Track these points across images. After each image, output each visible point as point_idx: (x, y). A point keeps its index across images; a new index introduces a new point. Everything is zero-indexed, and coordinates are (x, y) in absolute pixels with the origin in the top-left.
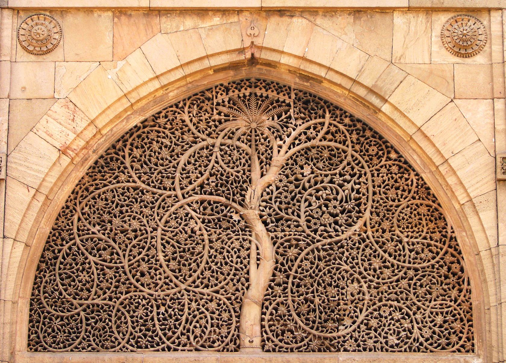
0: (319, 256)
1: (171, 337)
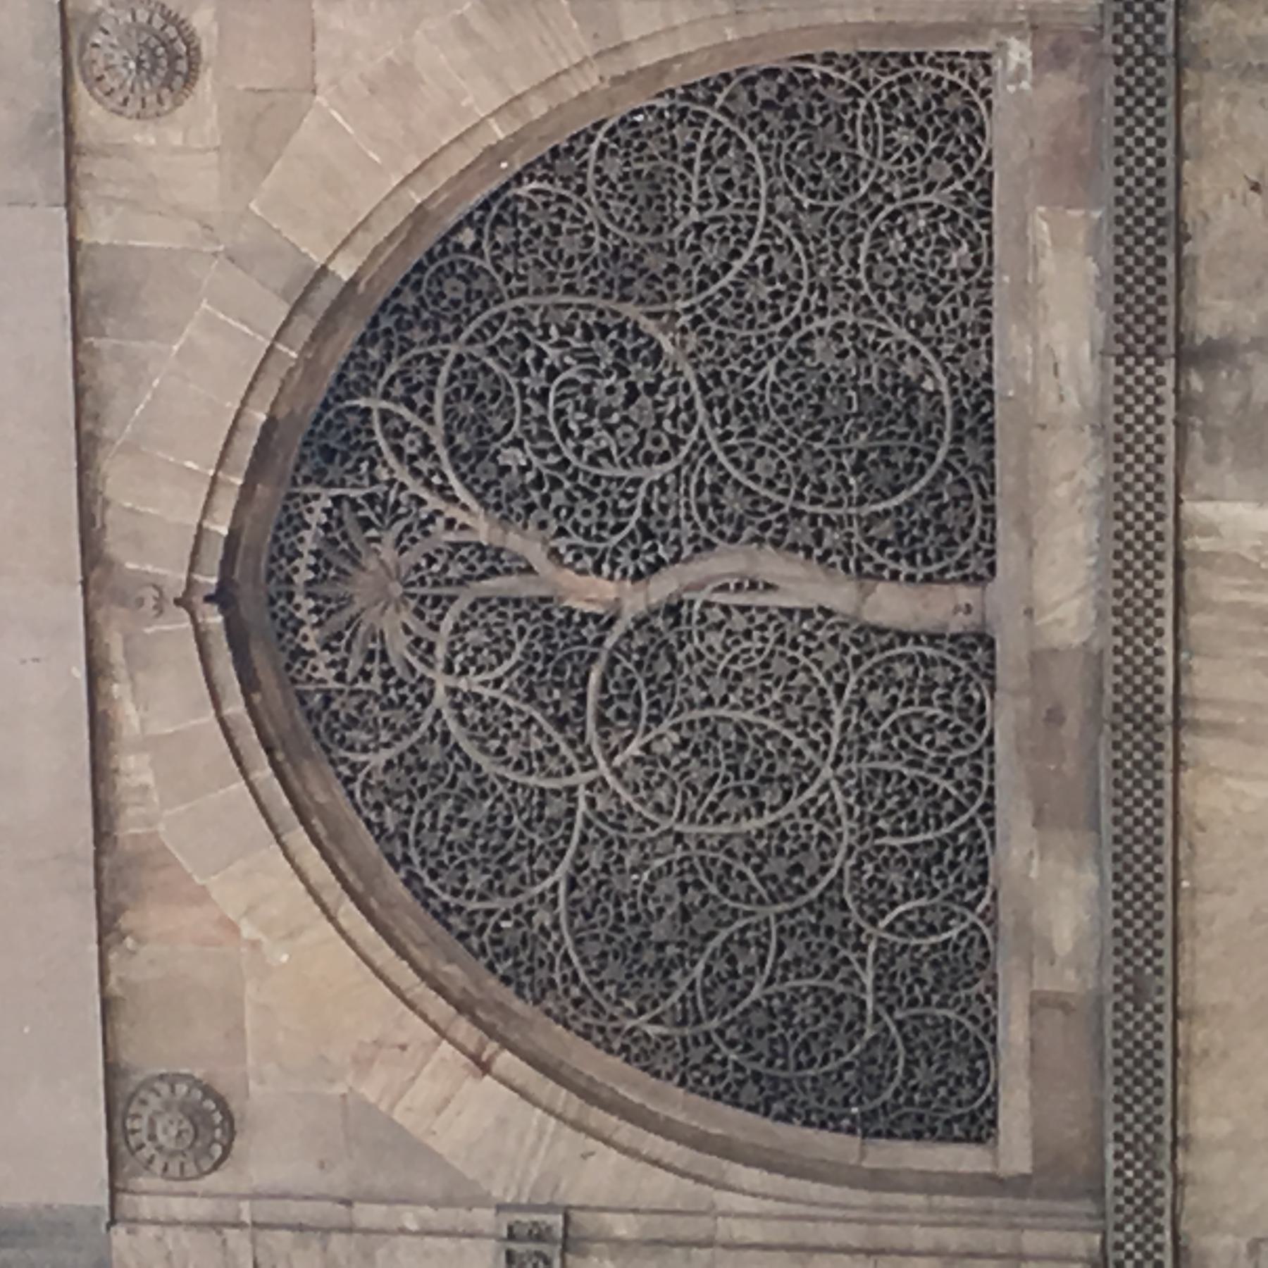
1: (958, 803)
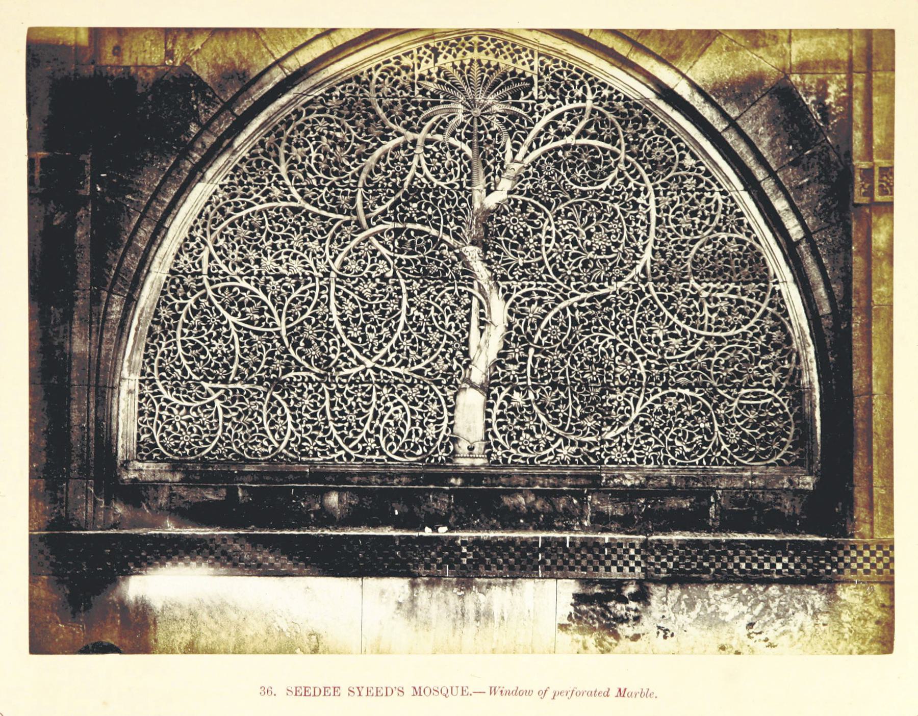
0: (573, 318)
1: (352, 440)
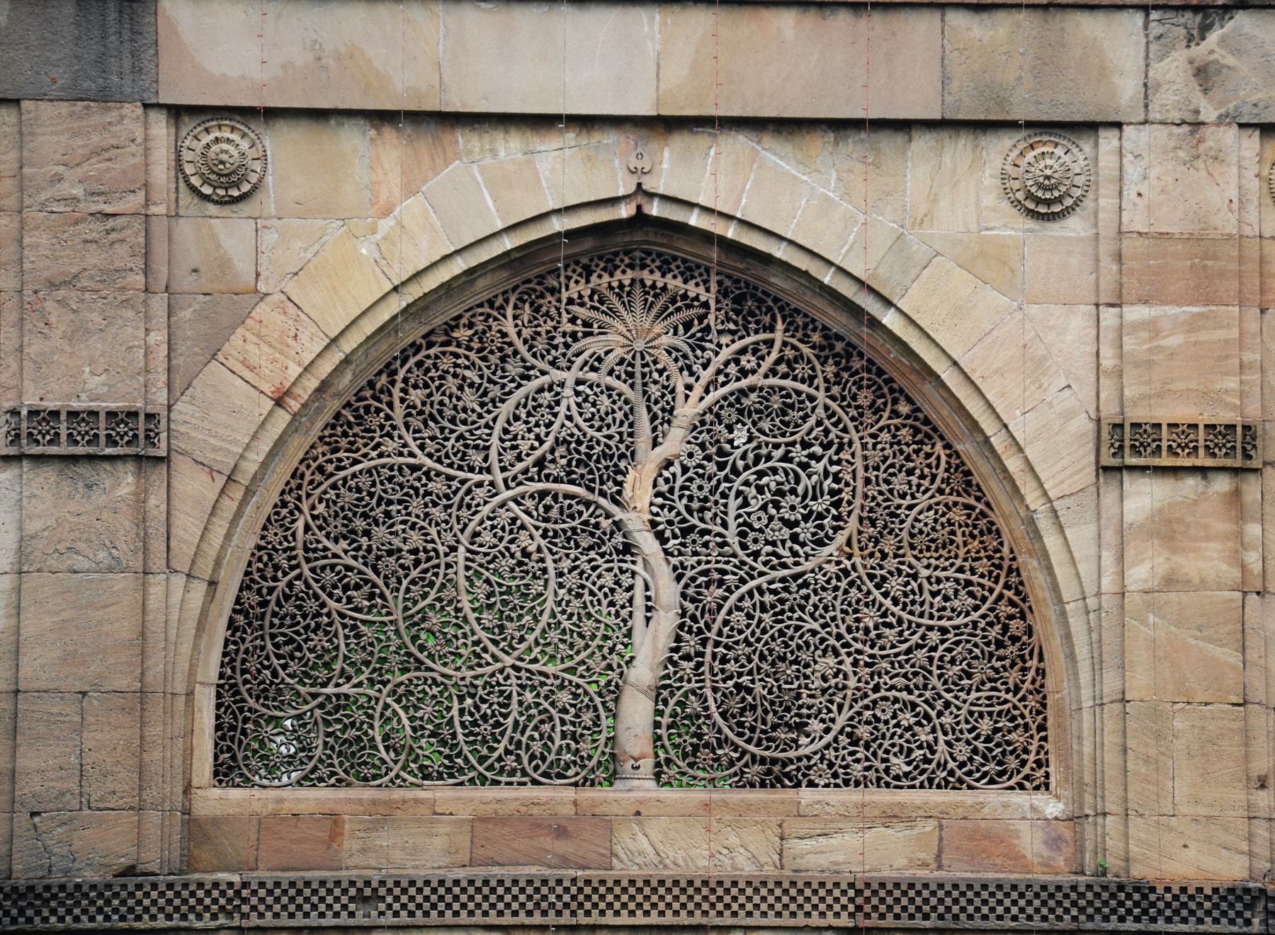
1: (487, 758)
